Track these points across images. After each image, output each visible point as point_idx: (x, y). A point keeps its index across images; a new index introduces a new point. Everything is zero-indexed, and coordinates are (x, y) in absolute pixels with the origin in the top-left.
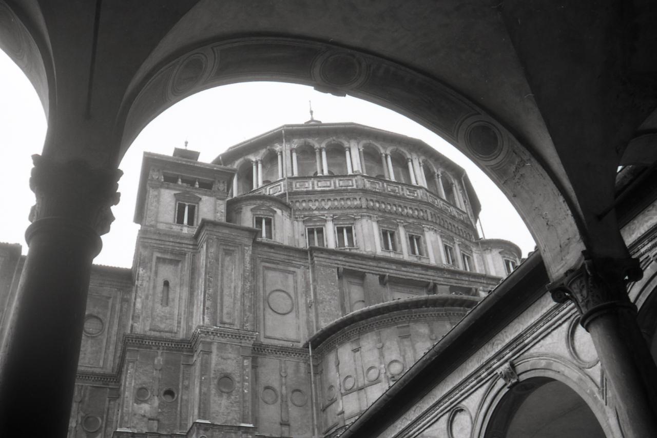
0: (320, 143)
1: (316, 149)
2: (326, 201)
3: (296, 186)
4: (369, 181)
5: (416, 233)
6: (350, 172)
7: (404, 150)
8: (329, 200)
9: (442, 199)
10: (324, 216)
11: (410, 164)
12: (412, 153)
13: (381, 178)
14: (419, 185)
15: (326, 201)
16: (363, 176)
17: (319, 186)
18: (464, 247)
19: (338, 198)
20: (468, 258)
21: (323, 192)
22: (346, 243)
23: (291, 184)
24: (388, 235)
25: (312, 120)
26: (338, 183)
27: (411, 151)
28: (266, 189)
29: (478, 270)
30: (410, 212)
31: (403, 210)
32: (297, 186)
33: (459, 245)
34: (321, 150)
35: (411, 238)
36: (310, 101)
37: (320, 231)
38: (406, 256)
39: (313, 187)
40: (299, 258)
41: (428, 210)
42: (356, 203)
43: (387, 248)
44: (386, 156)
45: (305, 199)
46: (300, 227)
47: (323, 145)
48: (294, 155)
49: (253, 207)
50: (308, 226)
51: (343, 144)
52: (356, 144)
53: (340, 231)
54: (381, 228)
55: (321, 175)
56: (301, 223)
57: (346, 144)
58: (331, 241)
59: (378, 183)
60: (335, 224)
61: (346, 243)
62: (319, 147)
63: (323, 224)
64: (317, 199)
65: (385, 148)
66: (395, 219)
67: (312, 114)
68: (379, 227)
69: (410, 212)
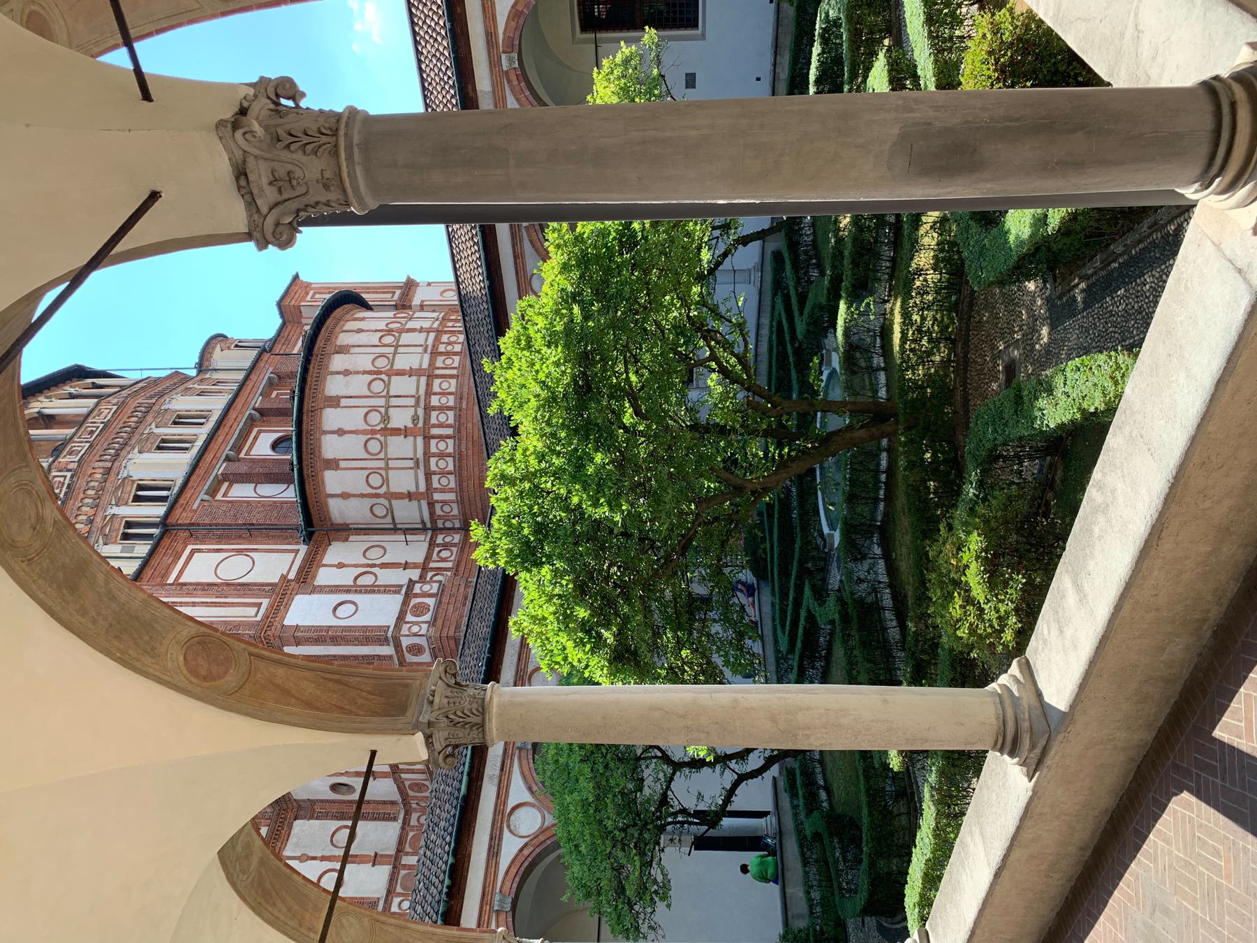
10: (106, 516)
14: (92, 406)
16: (54, 461)
19: (82, 495)
22: (164, 493)
29: (240, 376)
31: (129, 427)
35: (175, 423)
37: (129, 525)
38: (203, 433)
41: (140, 401)
42: (99, 476)
43: (187, 449)
53: (137, 499)
60: (126, 504)
61: (164, 493)
68: (149, 451)
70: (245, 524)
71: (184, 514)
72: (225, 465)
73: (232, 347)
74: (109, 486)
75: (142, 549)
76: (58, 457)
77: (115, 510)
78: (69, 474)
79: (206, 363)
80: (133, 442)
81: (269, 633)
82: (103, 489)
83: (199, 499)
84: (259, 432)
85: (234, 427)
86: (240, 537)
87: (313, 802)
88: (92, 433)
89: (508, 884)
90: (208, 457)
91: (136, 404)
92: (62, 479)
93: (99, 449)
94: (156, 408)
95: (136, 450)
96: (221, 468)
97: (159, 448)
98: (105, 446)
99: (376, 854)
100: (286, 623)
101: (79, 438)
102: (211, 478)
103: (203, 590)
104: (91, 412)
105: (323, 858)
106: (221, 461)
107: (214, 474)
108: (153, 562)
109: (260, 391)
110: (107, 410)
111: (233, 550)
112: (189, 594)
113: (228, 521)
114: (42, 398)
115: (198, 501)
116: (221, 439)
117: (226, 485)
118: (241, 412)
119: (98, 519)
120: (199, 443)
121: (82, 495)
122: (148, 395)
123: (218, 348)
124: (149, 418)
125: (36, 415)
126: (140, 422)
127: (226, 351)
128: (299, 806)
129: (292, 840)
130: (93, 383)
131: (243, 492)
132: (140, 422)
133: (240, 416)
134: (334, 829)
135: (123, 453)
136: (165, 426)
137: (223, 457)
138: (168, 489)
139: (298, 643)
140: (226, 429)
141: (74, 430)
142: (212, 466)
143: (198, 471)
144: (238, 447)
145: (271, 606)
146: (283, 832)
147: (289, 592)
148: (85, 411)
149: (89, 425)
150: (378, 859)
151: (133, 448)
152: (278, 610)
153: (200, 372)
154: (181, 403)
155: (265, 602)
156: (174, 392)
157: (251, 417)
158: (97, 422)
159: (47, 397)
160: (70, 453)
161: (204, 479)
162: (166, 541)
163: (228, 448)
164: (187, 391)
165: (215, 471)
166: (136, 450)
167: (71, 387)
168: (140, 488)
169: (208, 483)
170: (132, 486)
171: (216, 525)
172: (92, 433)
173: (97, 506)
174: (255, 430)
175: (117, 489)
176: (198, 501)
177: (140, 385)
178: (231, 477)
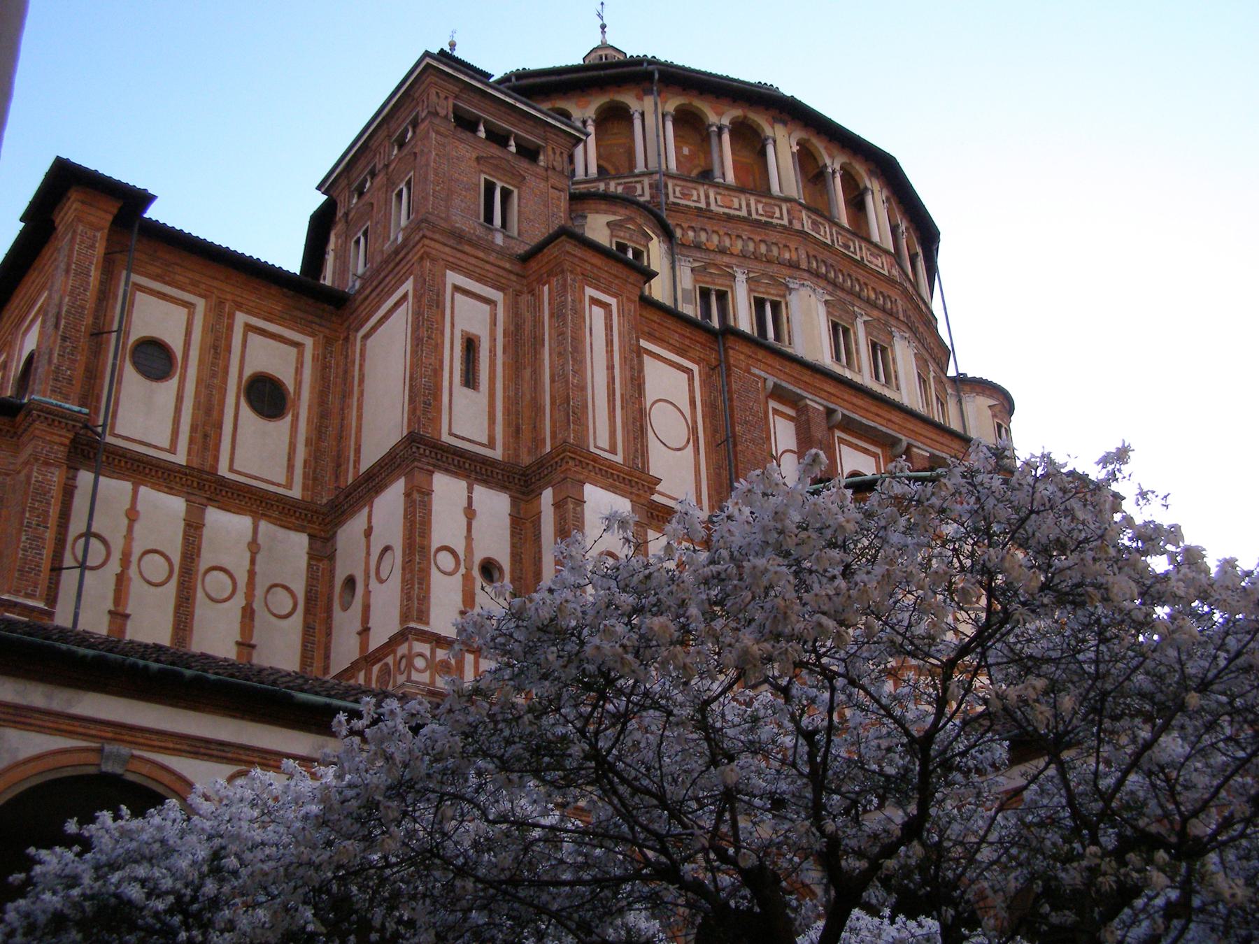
0: (720, 114)
1: (710, 126)
2: (733, 237)
3: (674, 193)
4: (809, 217)
5: (881, 339)
6: (775, 188)
7: (860, 169)
8: (739, 236)
9: (910, 280)
11: (869, 199)
12: (873, 179)
13: (822, 212)
14: (884, 246)
15: (733, 237)
16: (800, 204)
17: (716, 202)
18: (939, 382)
19: (757, 238)
20: (942, 405)
21: (729, 218)
23: (666, 186)
24: (839, 331)
25: (604, 46)
26: (754, 207)
27: (871, 173)
28: (607, 185)
30: (873, 296)
31: (861, 290)
32: (674, 192)
33: (934, 377)
34: (720, 129)
35: (874, 346)
36: (602, 4)
37: (722, 296)
38: (865, 378)
39: (708, 204)
40: (701, 343)
42: (787, 256)
43: (838, 359)
44: (834, 172)
45: (693, 225)
46: (686, 280)
47: (726, 121)
48: (669, 125)
49: (612, 218)
50: (704, 282)
51: (763, 130)
52: (787, 136)
53: (759, 304)
54: (830, 318)
55: (721, 181)
56: (688, 271)
57: (768, 131)
58: (744, 321)
59: (823, 225)
60: (750, 290)
62: (717, 123)
63: (728, 283)
64: (715, 229)
65: (832, 157)
66: (853, 305)
67: (603, 32)
68: (829, 313)
69: (873, 296)
70: (734, 435)
71: (742, 357)
72: (821, 408)
73: (996, 420)
74: (772, 269)
75: (691, 310)
76: (807, 208)
77: (741, 278)
78: (785, 222)
79: (967, 388)
80: (839, 293)
81: (571, 463)
82: (768, 261)
83: (766, 376)
84: (875, 455)
85: (878, 419)
86: (715, 431)
87: (332, 557)
88: (848, 247)
89: (145, 769)
90: (830, 387)
91: (894, 297)
92: (777, 214)
93: (825, 255)
94: (893, 322)
95: (828, 298)
96: (815, 403)
97: (835, 327)
98: (830, 261)
99: (253, 647)
100: (588, 488)
101: (838, 233)
102: (799, 391)
103: (632, 379)
104: (876, 246)
105: (252, 574)
106: (825, 403)
107: (805, 394)
108: (669, 322)
109: (937, 453)
110: (881, 264)
111: (695, 422)
112: (624, 360)
113: (738, 415)
114: (885, 193)
115: (763, 374)
116: (860, 402)
117: (792, 412)
118: (902, 428)
119: (726, 259)
120: (848, 374)
121: (757, 238)
122: (910, 313)
123: (992, 402)
124: (876, 313)
125: (862, 186)
126: (868, 301)
127: (989, 413)
128: (328, 540)
129: (281, 533)
130: (917, 254)
131: (784, 434)
132: (868, 301)
133: (896, 427)
134: (293, 587)
135: (823, 284)
136: (868, 334)
137: (832, 406)
138: (778, 337)
139: (558, 505)
140: (873, 409)
141: (847, 226)
142: (816, 391)
143: (807, 376)
144: (849, 426)
145: (612, 465)
146: (293, 520)
147: (634, 490)
148: (876, 238)
149: (855, 244)
150: (246, 650)
151: (830, 294)
152: (606, 474)
153: (953, 380)
154: (904, 355)
155: (619, 458)
156: (920, 346)
157: (895, 442)
158: (859, 251)
159: (888, 199)
160: (814, 223)
161: (797, 381)
162: (702, 338)
163: (846, 412)
164: (921, 361)
165: (810, 396)
166: (828, 298)
167: (907, 229)
168: (776, 307)
169: (791, 387)
170: (777, 295)
171: (731, 400)
172: (848, 247)
173: (744, 256)
174: (878, 451)
175: (771, 278)
176: (763, 374)
177: (923, 307)
178: (804, 418)
